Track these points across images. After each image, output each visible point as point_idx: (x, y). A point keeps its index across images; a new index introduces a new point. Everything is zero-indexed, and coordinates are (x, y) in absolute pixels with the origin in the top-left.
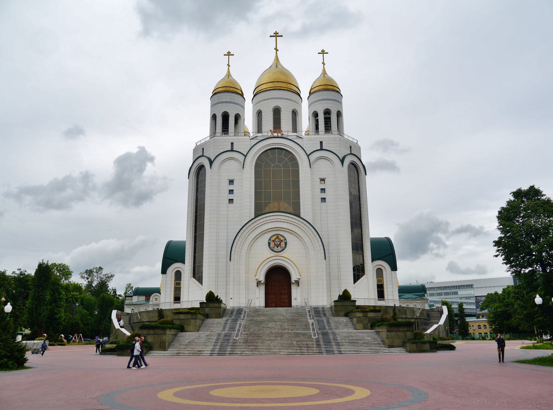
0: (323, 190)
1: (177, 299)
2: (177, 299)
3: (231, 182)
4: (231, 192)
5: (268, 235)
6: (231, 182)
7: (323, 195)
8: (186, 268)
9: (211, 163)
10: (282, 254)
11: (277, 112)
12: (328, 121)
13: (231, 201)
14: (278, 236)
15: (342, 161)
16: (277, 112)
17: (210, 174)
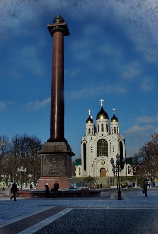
0: (113, 149)
1: (80, 174)
2: (80, 174)
3: (92, 147)
4: (92, 150)
5: (100, 161)
6: (92, 147)
7: (113, 150)
8: (82, 167)
9: (87, 143)
10: (104, 165)
11: (102, 125)
12: (115, 130)
13: (92, 152)
14: (103, 161)
15: (118, 142)
16: (102, 125)
17: (87, 146)
